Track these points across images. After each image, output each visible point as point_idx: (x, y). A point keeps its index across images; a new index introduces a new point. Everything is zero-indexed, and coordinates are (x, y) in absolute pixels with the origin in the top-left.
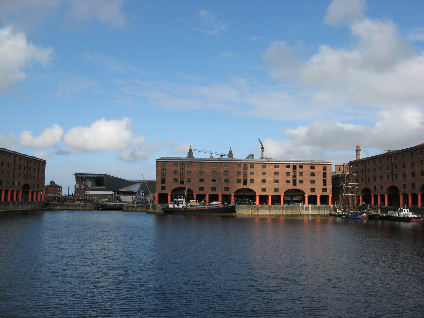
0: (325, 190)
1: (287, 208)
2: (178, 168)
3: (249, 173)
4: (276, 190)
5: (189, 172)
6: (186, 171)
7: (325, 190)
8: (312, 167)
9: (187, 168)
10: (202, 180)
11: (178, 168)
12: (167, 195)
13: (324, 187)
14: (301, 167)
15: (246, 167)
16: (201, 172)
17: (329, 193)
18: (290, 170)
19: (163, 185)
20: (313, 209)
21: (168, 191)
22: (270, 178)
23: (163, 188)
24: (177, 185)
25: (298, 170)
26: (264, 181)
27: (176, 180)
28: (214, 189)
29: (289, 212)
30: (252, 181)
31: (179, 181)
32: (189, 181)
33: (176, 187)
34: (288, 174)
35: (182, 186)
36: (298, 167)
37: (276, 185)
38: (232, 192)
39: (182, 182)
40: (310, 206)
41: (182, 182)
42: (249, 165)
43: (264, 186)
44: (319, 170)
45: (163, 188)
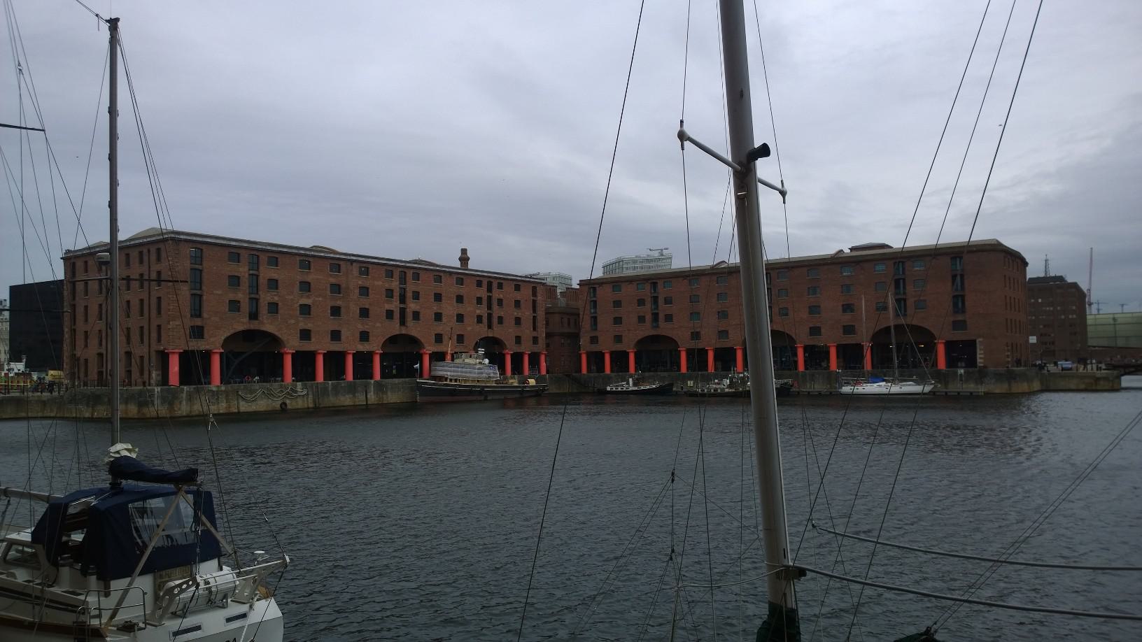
0: (535, 340)
2: (243, 270)
3: (409, 295)
5: (273, 284)
6: (263, 281)
7: (535, 340)
8: (517, 288)
9: (267, 272)
10: (306, 310)
11: (243, 270)
12: (207, 355)
13: (535, 334)
14: (500, 286)
15: (403, 280)
16: (306, 287)
17: (541, 347)
18: (482, 292)
19: (198, 322)
21: (214, 342)
22: (449, 309)
23: (198, 332)
24: (241, 323)
25: (496, 294)
27: (234, 305)
30: (416, 315)
31: (245, 307)
32: (274, 308)
33: (241, 328)
34: (479, 300)
35: (254, 326)
36: (495, 285)
39: (254, 316)
41: (254, 316)
42: (410, 274)
44: (526, 293)
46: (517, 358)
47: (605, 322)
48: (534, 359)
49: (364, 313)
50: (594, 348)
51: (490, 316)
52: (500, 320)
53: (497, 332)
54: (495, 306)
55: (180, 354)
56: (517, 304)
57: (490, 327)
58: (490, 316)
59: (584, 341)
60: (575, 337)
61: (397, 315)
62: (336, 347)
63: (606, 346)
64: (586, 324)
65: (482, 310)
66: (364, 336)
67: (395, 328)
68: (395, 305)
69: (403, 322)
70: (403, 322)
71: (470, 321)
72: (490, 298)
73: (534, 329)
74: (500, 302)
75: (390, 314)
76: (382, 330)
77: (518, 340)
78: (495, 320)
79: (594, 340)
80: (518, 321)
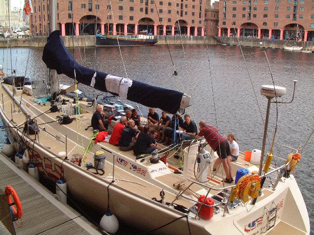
0: (200, 22)
1: (178, 38)
4: (169, 20)
13: (200, 19)
17: (202, 25)
19: (70, 12)
20: (194, 39)
21: (77, 20)
24: (86, 13)
26: (161, 11)
28: (121, 18)
29: (178, 42)
30: (152, 10)
31: (87, 7)
33: (85, 14)
35: (91, 13)
37: (169, 16)
38: (136, 22)
39: (90, 10)
40: (192, 36)
41: (90, 10)
43: (161, 16)
45: (70, 16)
46: (192, 29)
47: (229, 16)
48: (199, 30)
49: (132, 9)
50: (224, 26)
51: (182, 12)
52: (186, 13)
53: (184, 18)
54: (184, 7)
55: (65, 24)
56: (194, 7)
57: (182, 16)
58: (182, 12)
59: (220, 23)
60: (217, 21)
61: (144, 10)
62: (121, 22)
63: (229, 26)
64: (221, 16)
65: (179, 9)
66: (131, 18)
67: (143, 15)
68: (144, 6)
69: (147, 13)
70: (147, 13)
71: (174, 13)
72: (182, 4)
73: (200, 17)
74: (186, 6)
75: (141, 10)
76: (138, 16)
77: (193, 21)
78: (184, 13)
79: (224, 23)
80: (193, 14)
